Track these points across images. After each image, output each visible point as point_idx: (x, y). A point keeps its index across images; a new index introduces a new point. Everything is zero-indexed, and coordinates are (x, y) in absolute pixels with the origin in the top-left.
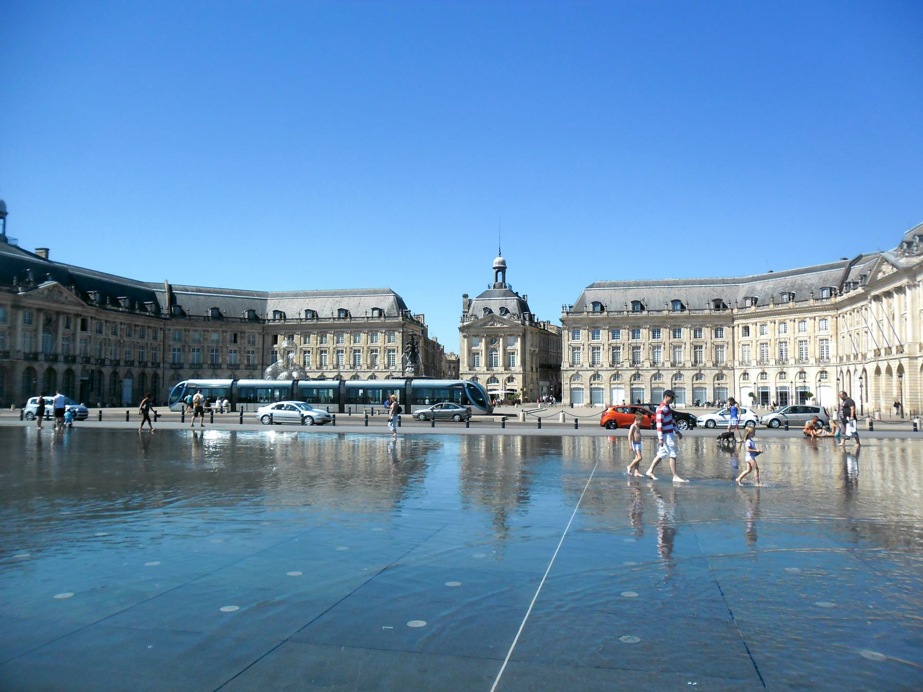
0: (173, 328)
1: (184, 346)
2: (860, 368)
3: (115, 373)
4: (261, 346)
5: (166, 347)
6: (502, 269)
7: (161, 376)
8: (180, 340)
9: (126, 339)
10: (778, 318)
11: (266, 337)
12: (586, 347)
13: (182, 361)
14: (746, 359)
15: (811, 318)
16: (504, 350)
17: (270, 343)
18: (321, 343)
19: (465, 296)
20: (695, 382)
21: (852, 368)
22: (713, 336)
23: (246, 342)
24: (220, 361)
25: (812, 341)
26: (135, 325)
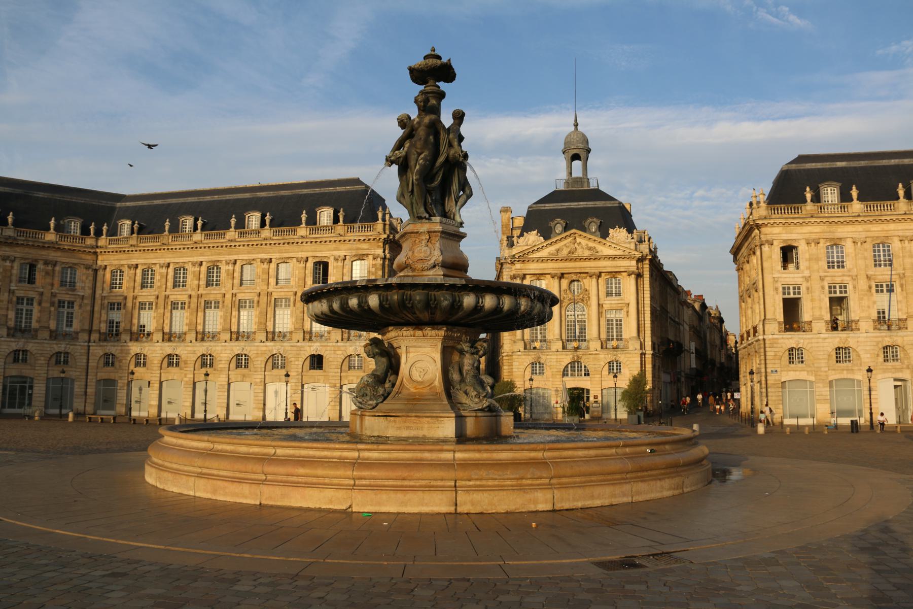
4: (88, 292)
16: (600, 306)
23: (57, 280)
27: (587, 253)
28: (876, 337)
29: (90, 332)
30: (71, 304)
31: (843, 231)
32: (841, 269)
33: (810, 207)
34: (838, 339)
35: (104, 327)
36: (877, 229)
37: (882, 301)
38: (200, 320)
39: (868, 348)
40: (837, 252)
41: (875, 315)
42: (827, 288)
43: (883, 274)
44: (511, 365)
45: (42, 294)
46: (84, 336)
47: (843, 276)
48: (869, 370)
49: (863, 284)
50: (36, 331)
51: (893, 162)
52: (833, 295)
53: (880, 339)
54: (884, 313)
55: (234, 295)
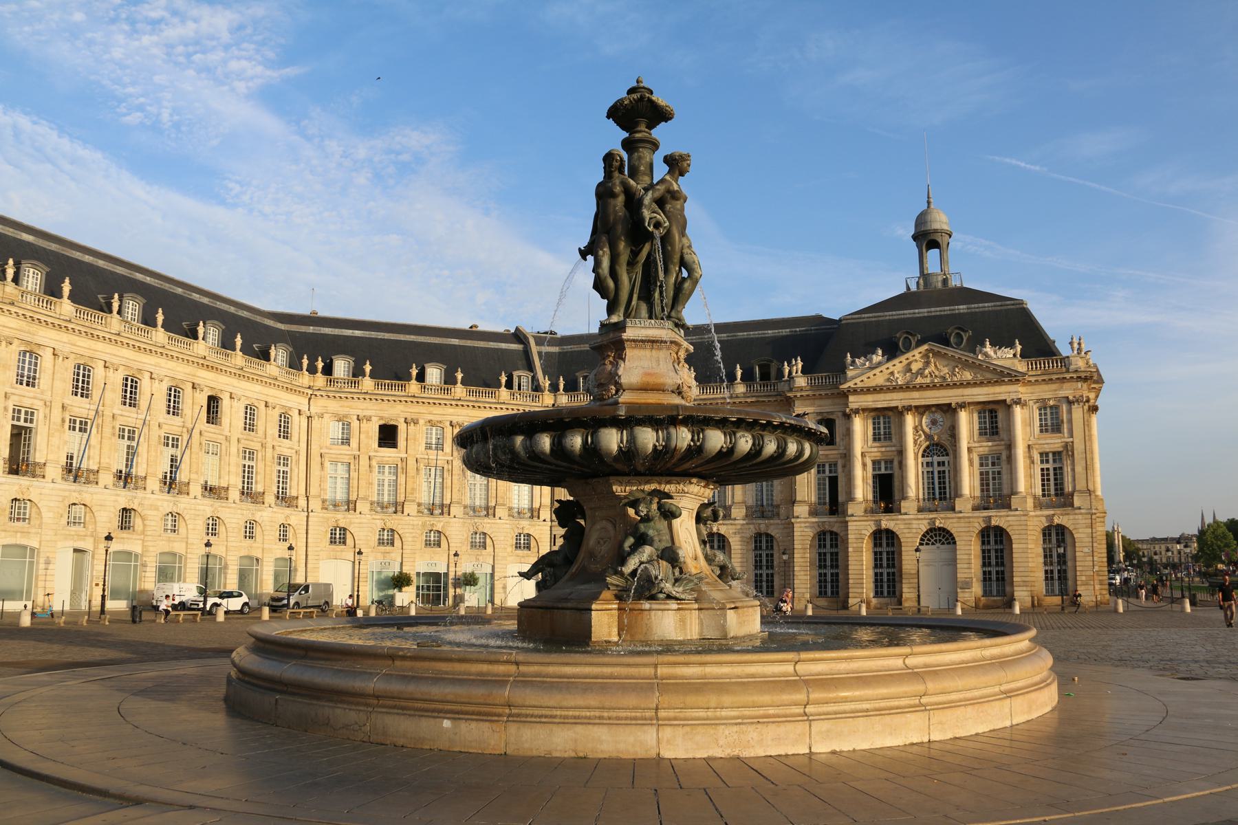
28: (64, 490)
31: (47, 336)
32: (30, 388)
34: (16, 488)
36: (84, 345)
37: (74, 441)
39: (52, 504)
40: (30, 363)
41: (63, 461)
42: (11, 411)
43: (81, 407)
47: (35, 398)
48: (109, 538)
49: (57, 414)
51: (87, 258)
52: (16, 423)
53: (67, 494)
54: (72, 458)
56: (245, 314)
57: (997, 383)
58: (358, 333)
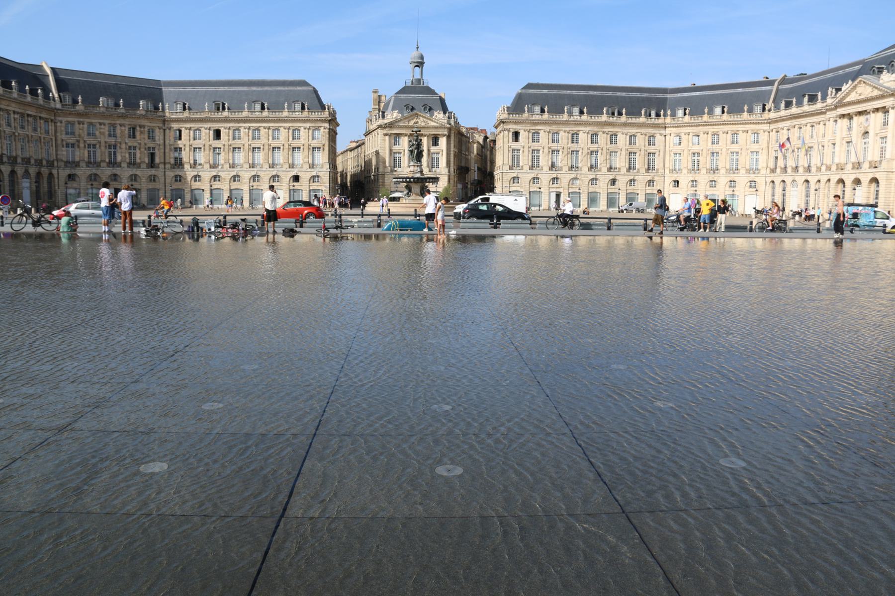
0: (64, 119)
1: (78, 141)
2: (800, 180)
3: (13, 173)
4: (162, 142)
5: (59, 142)
6: (420, 64)
7: (56, 176)
8: (73, 133)
9: (20, 131)
10: (712, 129)
11: (167, 131)
12: (526, 149)
13: (77, 159)
14: (677, 167)
15: (743, 132)
16: (429, 150)
17: (172, 140)
18: (234, 139)
19: (375, 92)
20: (628, 187)
21: (788, 180)
22: (647, 144)
23: (146, 137)
24: (119, 159)
25: (744, 153)
26: (28, 115)
27: (423, 124)
29: (165, 163)
30: (154, 148)
33: (526, 115)
35: (172, 161)
38: (231, 158)
41: (550, 164)
44: (384, 179)
45: (140, 144)
46: (162, 166)
49: (546, 150)
50: (140, 164)
55: (250, 145)
56: (645, 95)
57: (882, 97)
58: (698, 93)
